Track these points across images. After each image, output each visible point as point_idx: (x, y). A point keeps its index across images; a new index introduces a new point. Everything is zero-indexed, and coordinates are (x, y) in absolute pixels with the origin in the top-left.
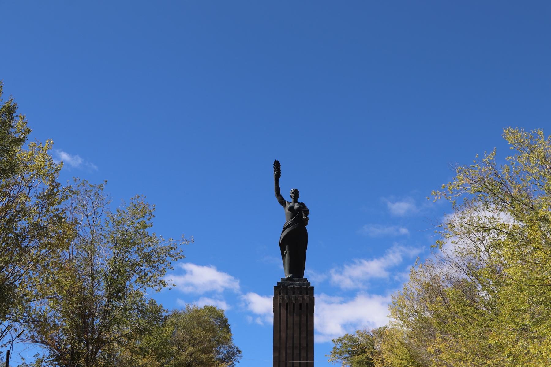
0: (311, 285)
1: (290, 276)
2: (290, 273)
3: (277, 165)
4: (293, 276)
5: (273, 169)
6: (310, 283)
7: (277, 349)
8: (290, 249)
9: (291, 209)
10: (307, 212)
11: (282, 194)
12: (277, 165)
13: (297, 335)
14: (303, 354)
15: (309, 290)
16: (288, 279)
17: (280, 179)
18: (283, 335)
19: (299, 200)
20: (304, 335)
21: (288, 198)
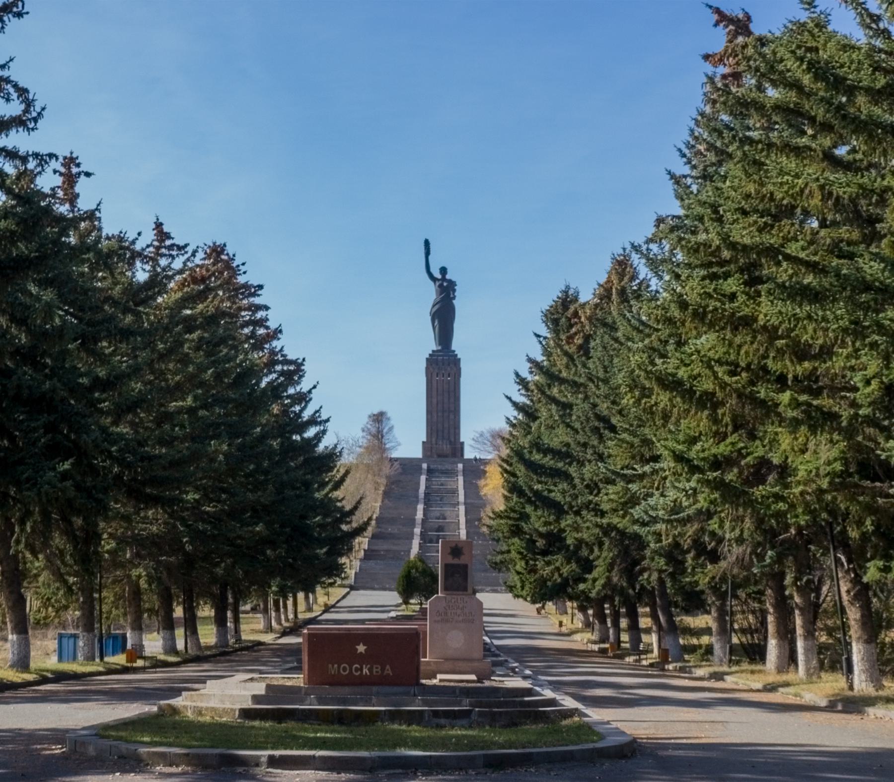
0: (459, 357)
1: (440, 348)
2: (440, 344)
3: (427, 243)
4: (443, 349)
5: (423, 248)
6: (456, 355)
7: (429, 412)
8: (439, 322)
9: (441, 286)
10: (454, 291)
11: (432, 270)
12: (427, 243)
13: (446, 400)
14: (452, 416)
15: (455, 362)
16: (437, 351)
17: (430, 257)
18: (435, 401)
19: (448, 277)
20: (452, 400)
21: (439, 276)
